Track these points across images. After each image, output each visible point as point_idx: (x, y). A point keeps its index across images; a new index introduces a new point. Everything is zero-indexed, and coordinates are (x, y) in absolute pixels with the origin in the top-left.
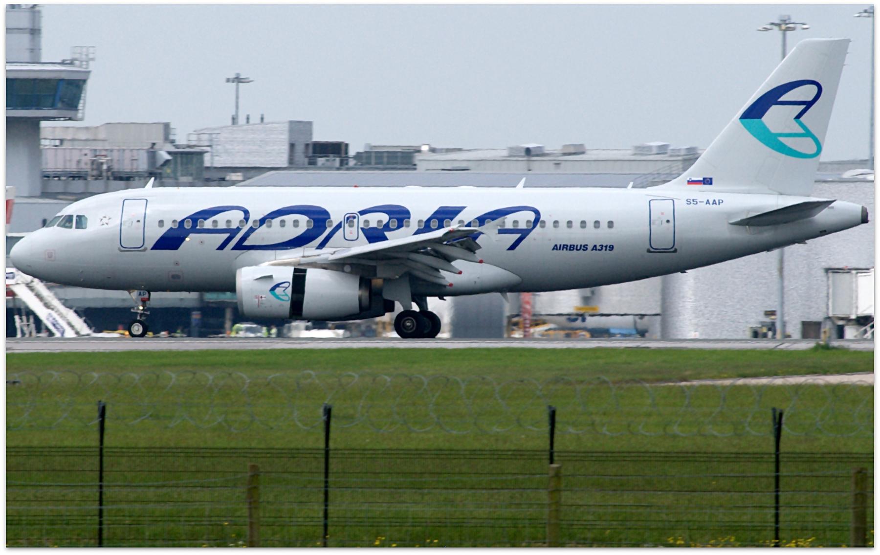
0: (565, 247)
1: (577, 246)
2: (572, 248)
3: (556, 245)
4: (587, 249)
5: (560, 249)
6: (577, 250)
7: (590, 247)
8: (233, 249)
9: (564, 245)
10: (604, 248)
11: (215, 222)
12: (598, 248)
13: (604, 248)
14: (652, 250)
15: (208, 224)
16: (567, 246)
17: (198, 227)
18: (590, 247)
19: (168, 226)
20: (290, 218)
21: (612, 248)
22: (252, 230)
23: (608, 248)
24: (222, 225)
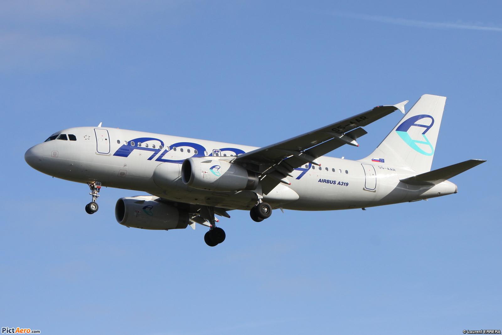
0: (324, 181)
1: (331, 181)
2: (328, 182)
3: (320, 179)
4: (335, 183)
5: (322, 182)
6: (330, 183)
7: (337, 183)
9: (324, 180)
10: (344, 184)
12: (341, 183)
13: (344, 184)
14: (365, 189)
15: (144, 145)
16: (326, 180)
17: (138, 146)
18: (337, 183)
20: (185, 148)
21: (347, 184)
22: (166, 151)
24: (150, 147)
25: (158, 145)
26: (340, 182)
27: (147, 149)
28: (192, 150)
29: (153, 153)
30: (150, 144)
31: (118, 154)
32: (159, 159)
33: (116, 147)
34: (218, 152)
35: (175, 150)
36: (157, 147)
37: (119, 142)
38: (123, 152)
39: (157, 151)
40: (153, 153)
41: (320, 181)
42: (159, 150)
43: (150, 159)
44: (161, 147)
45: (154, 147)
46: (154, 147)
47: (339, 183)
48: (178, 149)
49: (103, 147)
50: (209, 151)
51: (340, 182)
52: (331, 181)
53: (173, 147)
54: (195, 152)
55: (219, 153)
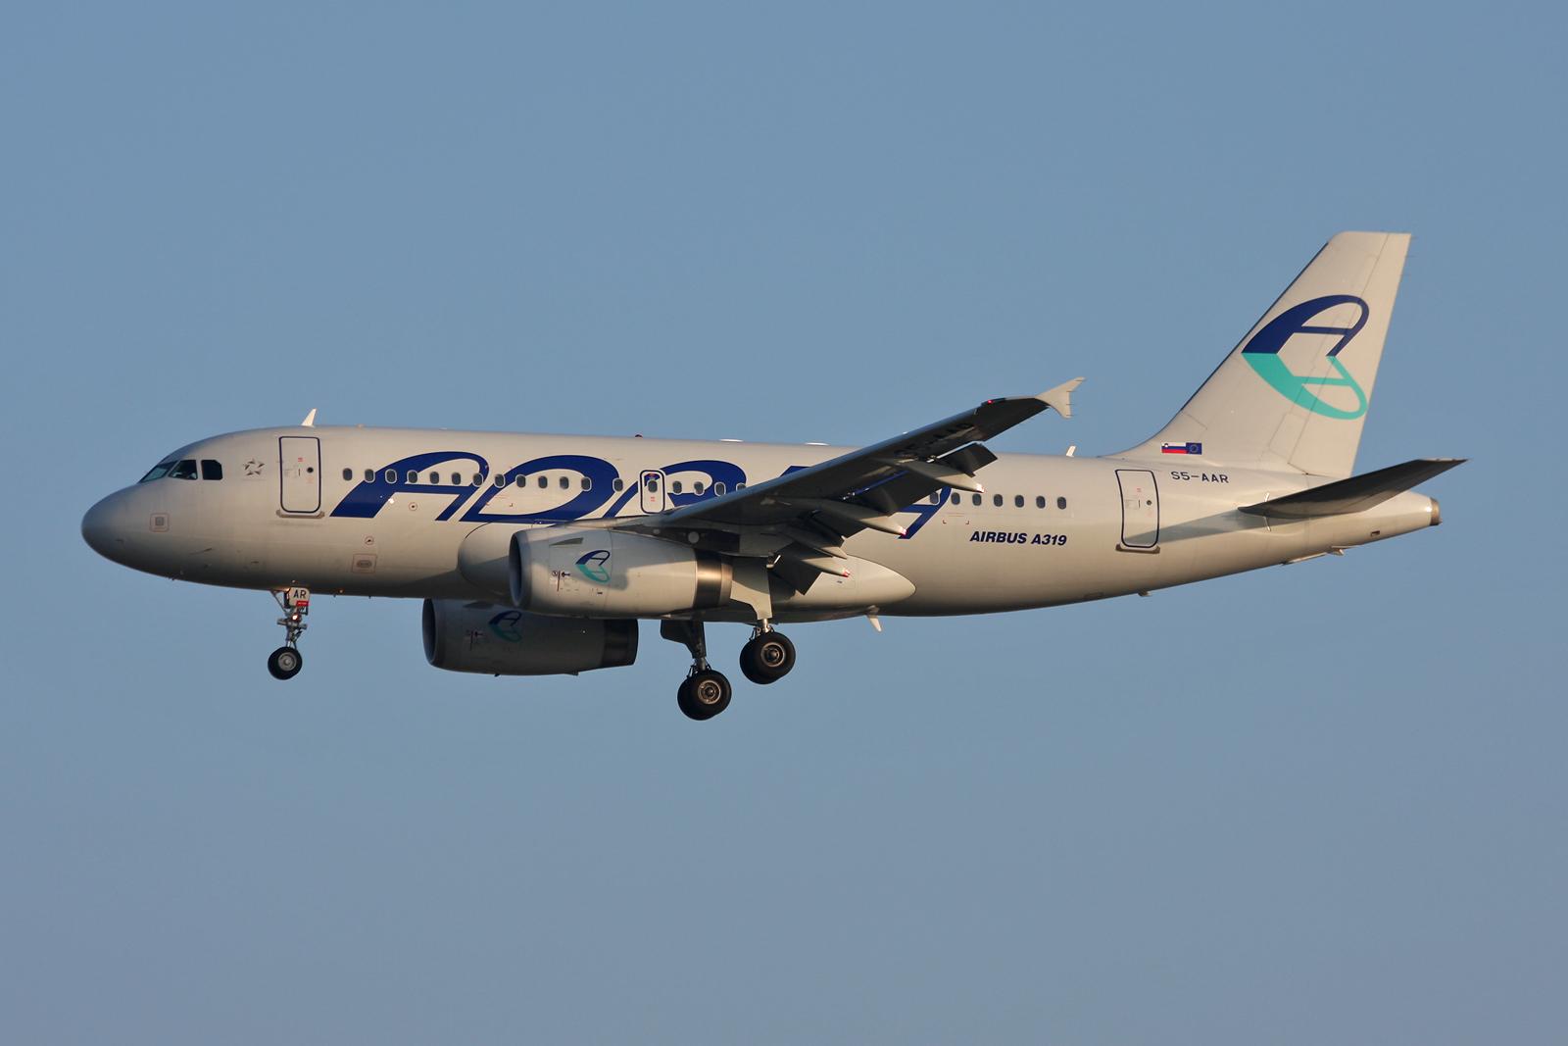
0: (991, 536)
1: (1010, 534)
2: (1002, 537)
3: (977, 533)
4: (1025, 540)
5: (982, 540)
6: (1009, 541)
7: (1030, 539)
8: (462, 520)
9: (989, 533)
10: (1052, 540)
11: (435, 477)
12: (1042, 539)
13: (1052, 540)
14: (1123, 547)
15: (423, 477)
16: (994, 534)
17: (408, 482)
19: (359, 478)
20: (554, 475)
21: (1063, 540)
22: (492, 492)
23: (1058, 541)
24: (445, 480)
25: (468, 470)
26: (1038, 536)
27: (434, 489)
28: (576, 477)
29: (452, 498)
30: (445, 471)
31: (345, 509)
32: (473, 515)
33: (338, 491)
34: (657, 477)
35: (522, 483)
36: (466, 481)
37: (348, 474)
38: (363, 502)
39: (465, 493)
40: (452, 498)
41: (976, 537)
42: (471, 490)
43: (445, 516)
44: (479, 479)
45: (456, 477)
46: (456, 477)
47: (1037, 539)
48: (532, 479)
49: (301, 492)
50: (628, 477)
51: (1038, 536)
52: (1010, 534)
53: (517, 475)
54: (584, 483)
55: (659, 482)
